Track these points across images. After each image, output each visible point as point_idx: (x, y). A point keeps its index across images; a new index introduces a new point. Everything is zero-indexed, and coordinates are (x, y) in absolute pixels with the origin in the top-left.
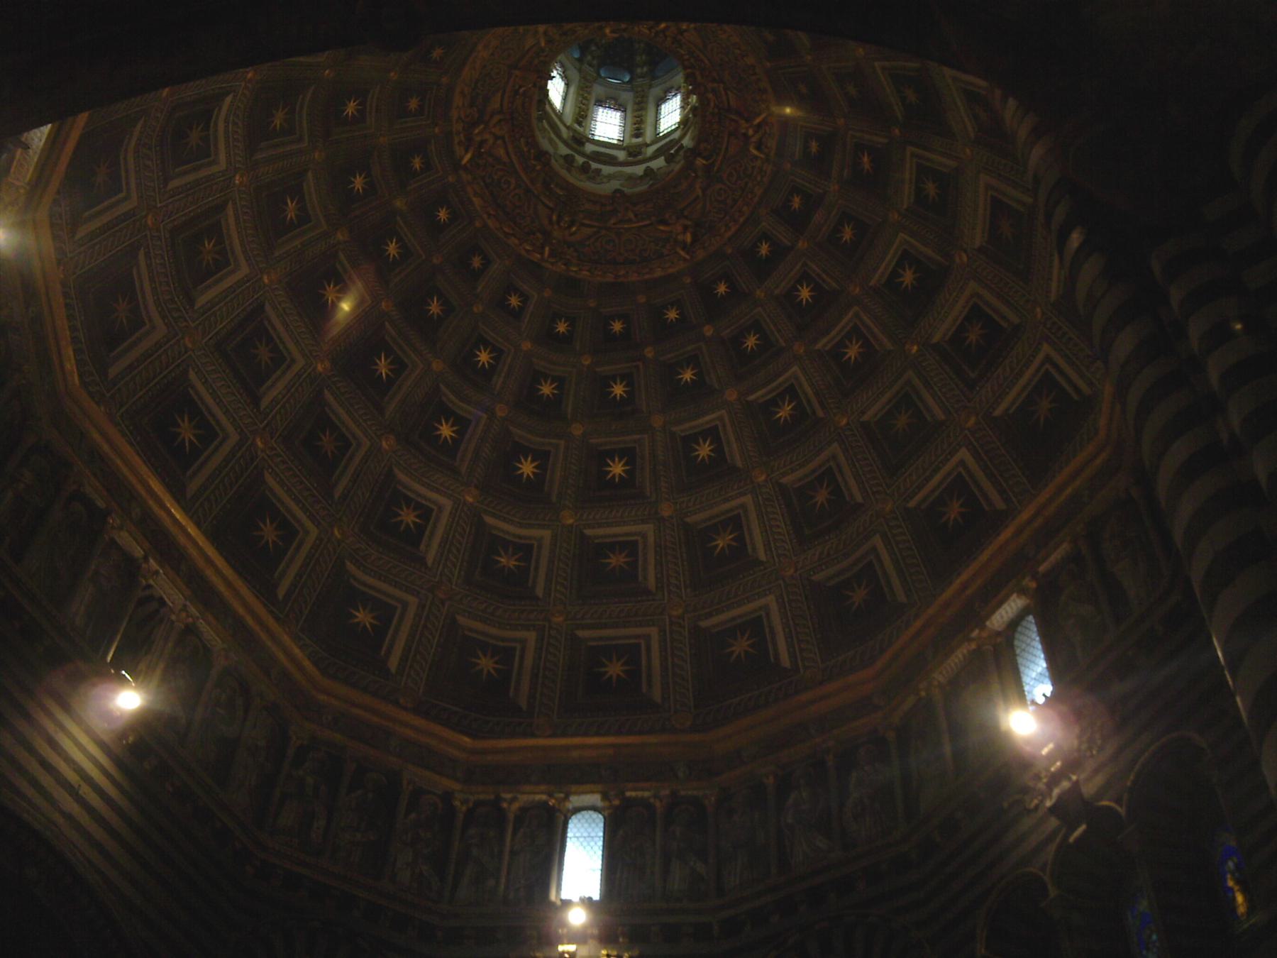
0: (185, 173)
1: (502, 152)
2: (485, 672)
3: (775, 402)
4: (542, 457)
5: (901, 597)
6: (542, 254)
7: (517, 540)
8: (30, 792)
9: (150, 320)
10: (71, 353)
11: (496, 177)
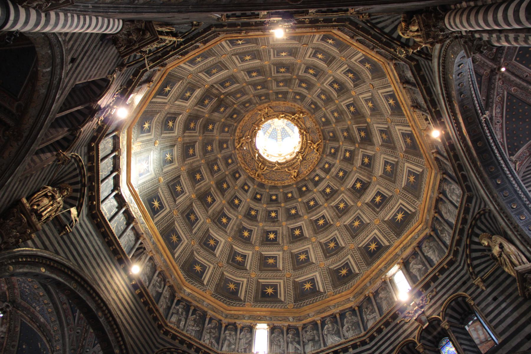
0: (166, 133)
4: (250, 231)
5: (357, 271)
8: (104, 288)
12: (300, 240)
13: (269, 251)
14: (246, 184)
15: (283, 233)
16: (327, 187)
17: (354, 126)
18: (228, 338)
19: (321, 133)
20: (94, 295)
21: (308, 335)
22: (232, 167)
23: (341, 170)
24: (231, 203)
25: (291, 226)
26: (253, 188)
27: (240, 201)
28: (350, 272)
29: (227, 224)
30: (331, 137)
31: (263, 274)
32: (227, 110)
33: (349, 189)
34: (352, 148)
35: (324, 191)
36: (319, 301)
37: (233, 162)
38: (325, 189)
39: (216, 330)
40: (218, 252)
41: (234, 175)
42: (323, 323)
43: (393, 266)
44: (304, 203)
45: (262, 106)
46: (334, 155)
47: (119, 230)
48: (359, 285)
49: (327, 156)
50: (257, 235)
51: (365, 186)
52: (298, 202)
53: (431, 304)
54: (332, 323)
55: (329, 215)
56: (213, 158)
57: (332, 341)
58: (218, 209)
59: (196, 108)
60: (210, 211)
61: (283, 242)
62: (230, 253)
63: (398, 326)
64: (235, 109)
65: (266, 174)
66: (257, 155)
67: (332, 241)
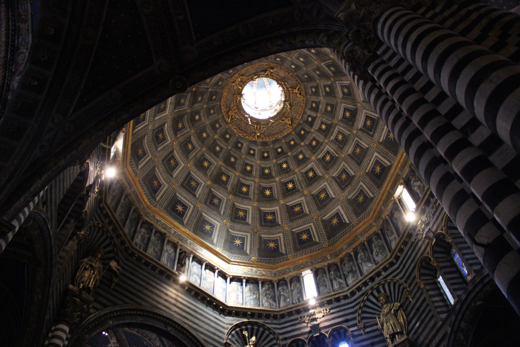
0: (161, 146)
4: (270, 189)
8: (164, 308)
12: (315, 181)
13: (293, 201)
14: (250, 149)
15: (298, 179)
16: (321, 124)
17: (322, 64)
18: (282, 293)
19: (297, 78)
20: (159, 317)
21: (347, 268)
22: (232, 141)
23: (327, 105)
24: (244, 172)
25: (304, 171)
26: (259, 149)
27: (252, 166)
28: (366, 197)
29: (248, 192)
30: (306, 78)
31: (295, 224)
32: (205, 97)
33: (341, 120)
34: (330, 82)
35: (320, 128)
36: (348, 232)
37: (231, 136)
38: (320, 126)
39: (271, 290)
40: (249, 220)
41: (236, 147)
42: (356, 254)
43: (398, 187)
44: (307, 145)
45: (233, 78)
46: (316, 93)
47: (157, 252)
48: (376, 209)
49: (311, 96)
50: (277, 190)
51: (354, 113)
52: (301, 146)
53: (434, 220)
54: (363, 251)
55: (332, 148)
56: (212, 141)
57: (367, 268)
58: (235, 182)
59: (176, 111)
60: (229, 188)
61: (302, 188)
62: (260, 216)
63: (414, 245)
64: (211, 92)
65: (264, 132)
66: (249, 119)
67: (342, 172)
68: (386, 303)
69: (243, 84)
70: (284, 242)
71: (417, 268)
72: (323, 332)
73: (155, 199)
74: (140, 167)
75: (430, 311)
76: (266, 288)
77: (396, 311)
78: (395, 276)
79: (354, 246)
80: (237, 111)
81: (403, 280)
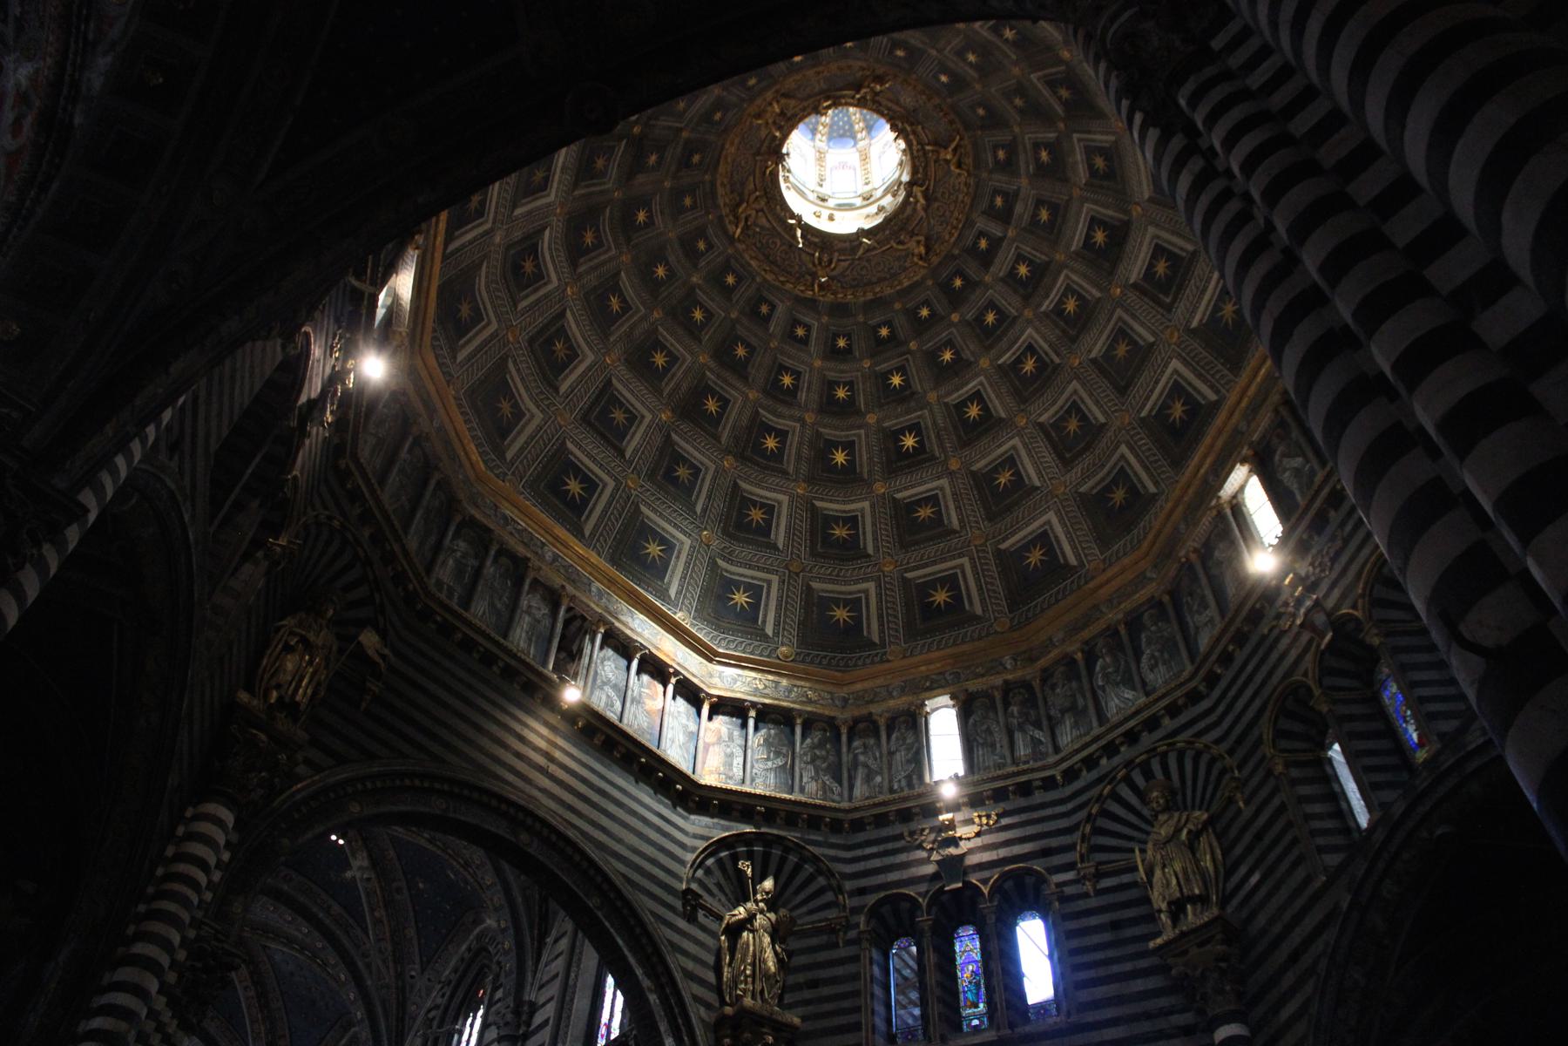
0: (527, 296)
1: (764, 220)
2: (841, 621)
3: (1019, 361)
4: (849, 447)
5: (1152, 489)
6: (813, 290)
7: (844, 515)
8: (511, 778)
9: (529, 410)
10: (474, 448)
11: (764, 241)
13: (913, 487)
14: (796, 323)
15: (935, 423)
18: (862, 758)
23: (1039, 203)
24: (774, 390)
25: (953, 398)
28: (1134, 492)
30: (982, 118)
33: (1077, 253)
34: (1052, 135)
35: (1012, 273)
37: (739, 279)
38: (1014, 268)
39: (828, 746)
40: (780, 536)
41: (754, 313)
44: (968, 323)
45: (759, 101)
46: (1009, 166)
48: (1159, 532)
49: (991, 172)
51: (1119, 235)
52: (952, 324)
53: (1334, 575)
57: (1120, 702)
58: (745, 421)
63: (1267, 643)
66: (799, 233)
67: (1068, 412)
68: (1167, 809)
69: (788, 123)
70: (879, 608)
71: (1267, 714)
72: (973, 879)
73: (501, 455)
74: (461, 356)
75: (1295, 841)
76: (816, 740)
77: (1195, 836)
78: (1199, 734)
79: (1086, 634)
80: (763, 203)
81: (1225, 746)
